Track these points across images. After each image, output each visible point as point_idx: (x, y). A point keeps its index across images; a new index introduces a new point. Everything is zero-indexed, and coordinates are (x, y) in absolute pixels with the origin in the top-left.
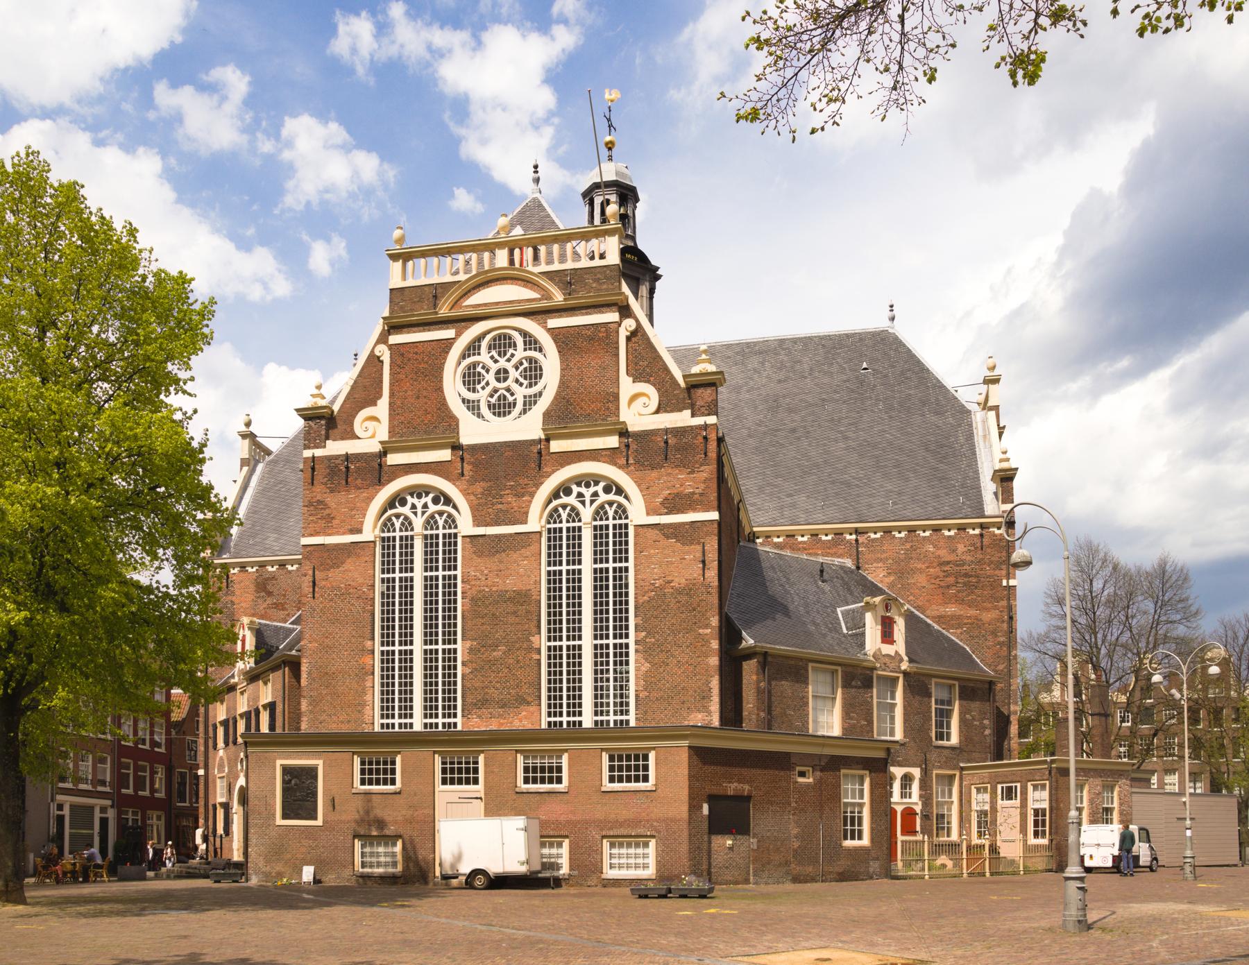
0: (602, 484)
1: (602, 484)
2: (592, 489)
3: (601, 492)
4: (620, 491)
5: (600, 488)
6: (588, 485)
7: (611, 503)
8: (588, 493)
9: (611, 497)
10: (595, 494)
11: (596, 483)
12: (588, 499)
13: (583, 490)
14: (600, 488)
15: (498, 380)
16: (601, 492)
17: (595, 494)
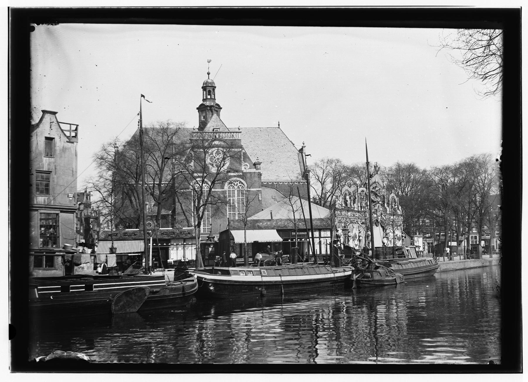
0: (239, 182)
1: (239, 182)
2: (237, 183)
3: (238, 183)
4: (242, 183)
5: (238, 183)
6: (236, 182)
7: (240, 186)
8: (236, 183)
9: (240, 184)
10: (237, 184)
11: (238, 182)
12: (236, 185)
13: (235, 183)
14: (238, 183)
15: (217, 160)
16: (238, 183)
17: (237, 184)
